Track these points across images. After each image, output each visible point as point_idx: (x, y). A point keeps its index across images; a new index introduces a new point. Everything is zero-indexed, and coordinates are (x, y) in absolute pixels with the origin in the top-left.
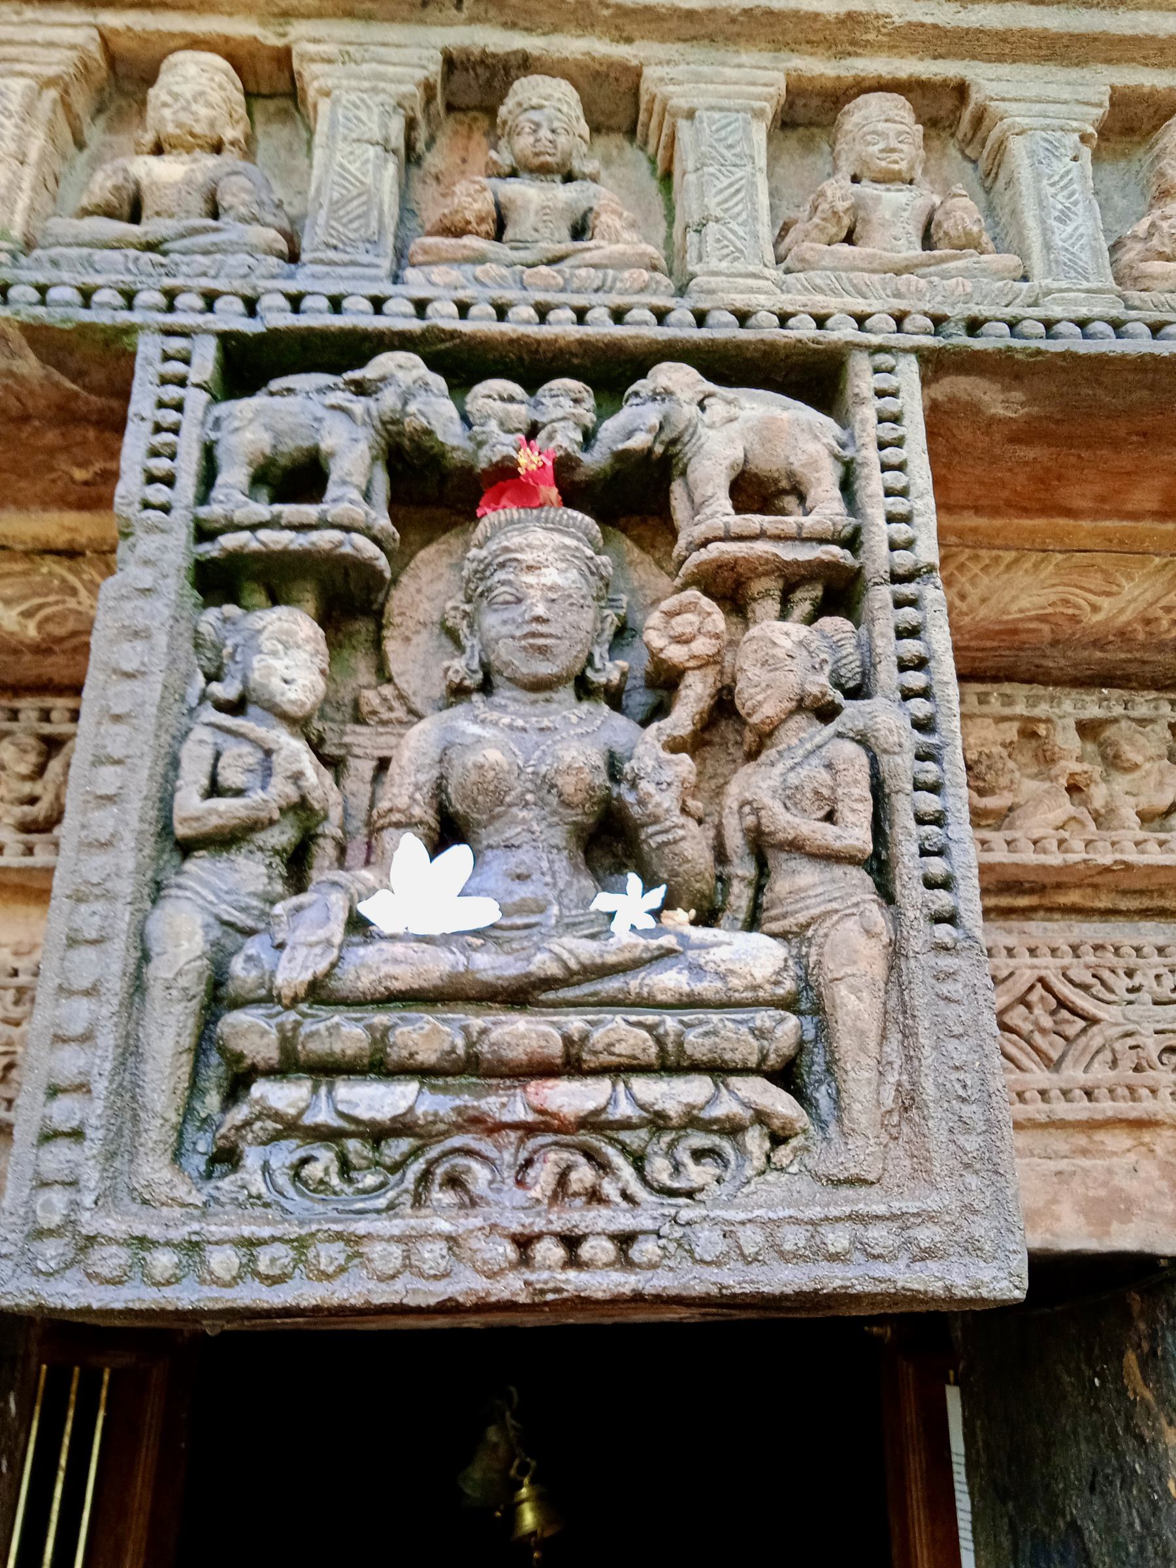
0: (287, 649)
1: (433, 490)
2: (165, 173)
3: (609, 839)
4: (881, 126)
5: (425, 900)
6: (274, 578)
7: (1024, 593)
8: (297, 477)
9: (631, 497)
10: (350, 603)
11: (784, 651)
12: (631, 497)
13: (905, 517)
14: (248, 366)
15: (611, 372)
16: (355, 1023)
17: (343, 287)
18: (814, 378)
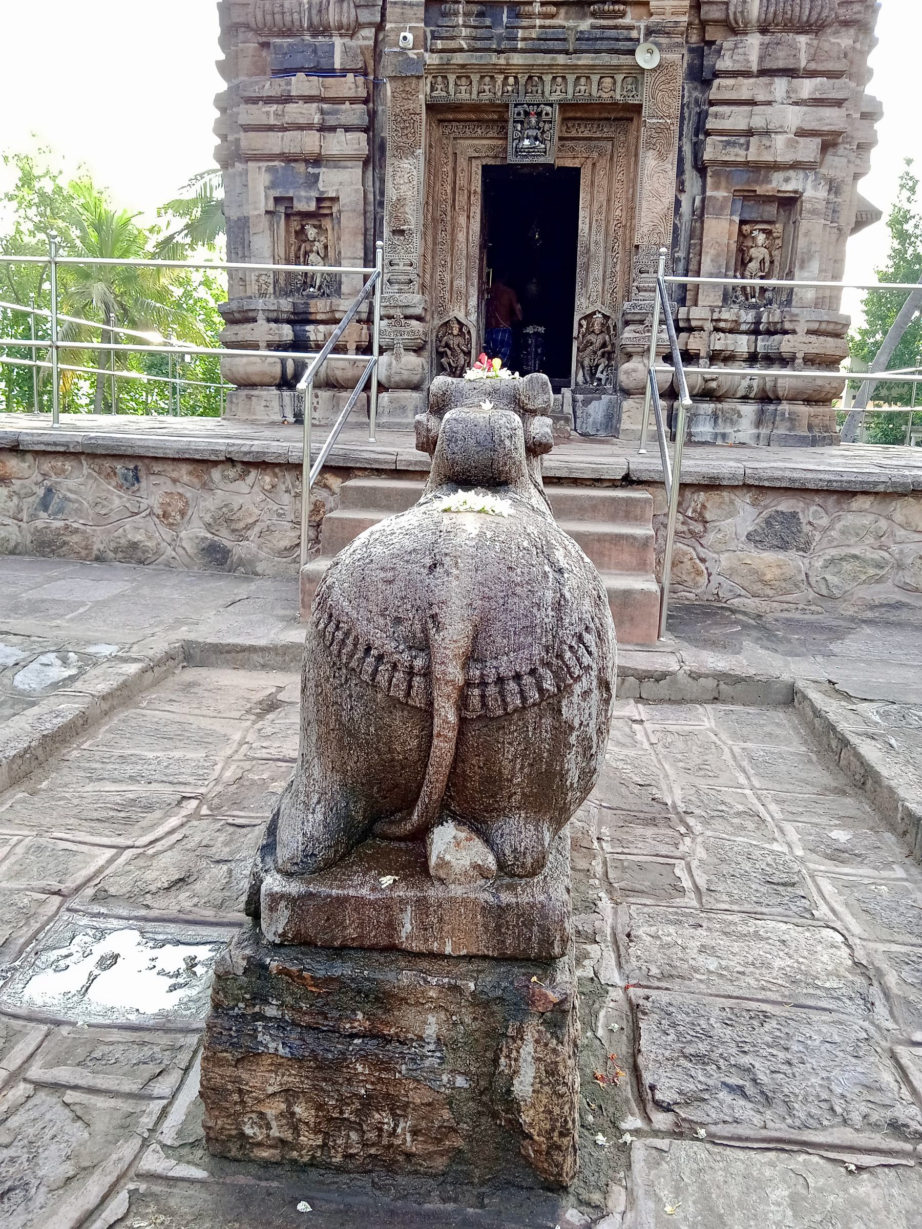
0: (519, 127)
1: (527, 114)
2: (510, 88)
3: (536, 139)
4: (559, 80)
5: (526, 142)
6: (517, 122)
7: (571, 115)
8: (519, 114)
9: (539, 114)
10: (522, 122)
11: (547, 126)
12: (539, 114)
13: (557, 117)
14: (516, 105)
15: (538, 105)
16: (522, 150)
17: (521, 99)
18: (551, 105)
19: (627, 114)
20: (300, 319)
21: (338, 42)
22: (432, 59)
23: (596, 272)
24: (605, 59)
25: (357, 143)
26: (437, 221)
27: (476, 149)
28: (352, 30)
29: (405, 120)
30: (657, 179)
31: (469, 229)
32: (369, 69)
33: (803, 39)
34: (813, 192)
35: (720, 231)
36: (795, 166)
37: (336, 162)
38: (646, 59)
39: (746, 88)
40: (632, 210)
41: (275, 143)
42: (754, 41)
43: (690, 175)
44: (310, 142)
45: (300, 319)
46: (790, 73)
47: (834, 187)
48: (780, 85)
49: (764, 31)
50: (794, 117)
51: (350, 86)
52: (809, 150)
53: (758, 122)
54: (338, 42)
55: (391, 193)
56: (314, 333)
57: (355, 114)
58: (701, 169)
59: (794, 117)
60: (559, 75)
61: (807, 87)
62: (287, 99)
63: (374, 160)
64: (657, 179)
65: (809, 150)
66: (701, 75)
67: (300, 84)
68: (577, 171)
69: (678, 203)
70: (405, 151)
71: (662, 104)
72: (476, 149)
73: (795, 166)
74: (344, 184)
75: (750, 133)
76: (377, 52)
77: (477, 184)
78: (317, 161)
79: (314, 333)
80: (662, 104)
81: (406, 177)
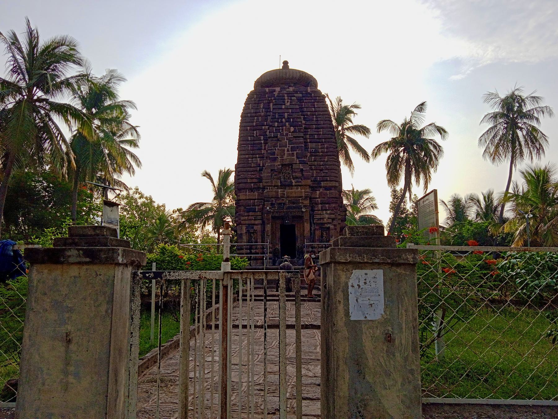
19: (301, 218)
20: (251, 248)
21: (257, 207)
22: (272, 211)
23: (299, 240)
24: (297, 210)
25: (260, 222)
26: (273, 233)
27: (279, 222)
28: (259, 205)
29: (268, 220)
30: (307, 226)
31: (278, 234)
32: (262, 210)
33: (327, 205)
34: (332, 227)
35: (318, 233)
36: (329, 223)
37: (257, 225)
38: (304, 210)
39: (320, 212)
40: (304, 231)
41: (247, 222)
42: (320, 206)
43: (313, 224)
44: (253, 222)
45: (251, 248)
46: (326, 210)
47: (335, 225)
48: (324, 212)
49: (321, 204)
50: (327, 216)
51: (259, 213)
52: (330, 221)
53: (322, 217)
54: (257, 207)
55: (266, 230)
56: (253, 251)
57: (259, 217)
58: (314, 224)
59: (327, 216)
60: (291, 212)
61: (328, 212)
62: (248, 216)
63: (263, 224)
64: (307, 226)
65: (330, 221)
66: (313, 210)
67: (251, 213)
68: (295, 225)
69: (311, 229)
70: (268, 224)
71: (306, 217)
72: (279, 222)
73: (329, 223)
74: (258, 228)
75: (321, 219)
76: (263, 208)
77: (279, 227)
78: (254, 224)
79: (253, 251)
80: (306, 217)
81: (268, 227)
